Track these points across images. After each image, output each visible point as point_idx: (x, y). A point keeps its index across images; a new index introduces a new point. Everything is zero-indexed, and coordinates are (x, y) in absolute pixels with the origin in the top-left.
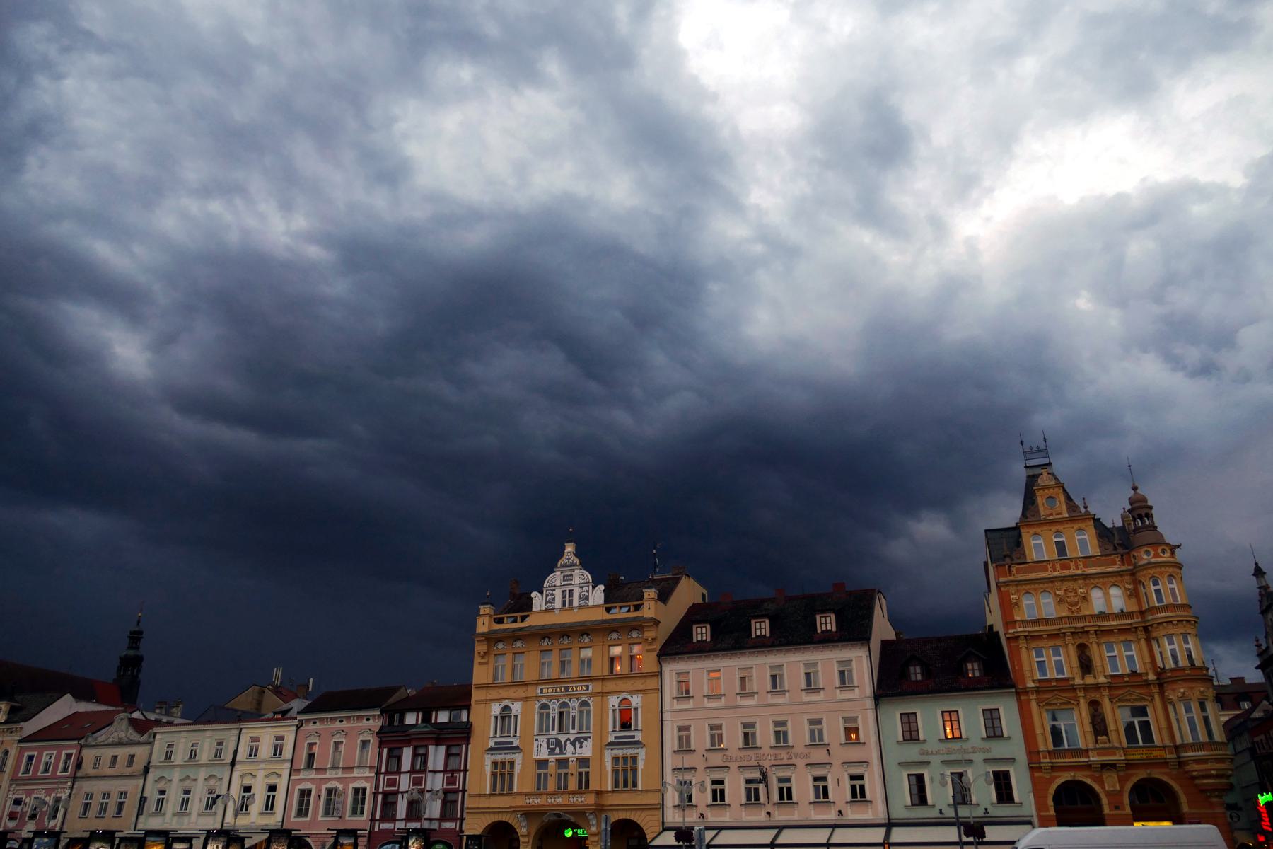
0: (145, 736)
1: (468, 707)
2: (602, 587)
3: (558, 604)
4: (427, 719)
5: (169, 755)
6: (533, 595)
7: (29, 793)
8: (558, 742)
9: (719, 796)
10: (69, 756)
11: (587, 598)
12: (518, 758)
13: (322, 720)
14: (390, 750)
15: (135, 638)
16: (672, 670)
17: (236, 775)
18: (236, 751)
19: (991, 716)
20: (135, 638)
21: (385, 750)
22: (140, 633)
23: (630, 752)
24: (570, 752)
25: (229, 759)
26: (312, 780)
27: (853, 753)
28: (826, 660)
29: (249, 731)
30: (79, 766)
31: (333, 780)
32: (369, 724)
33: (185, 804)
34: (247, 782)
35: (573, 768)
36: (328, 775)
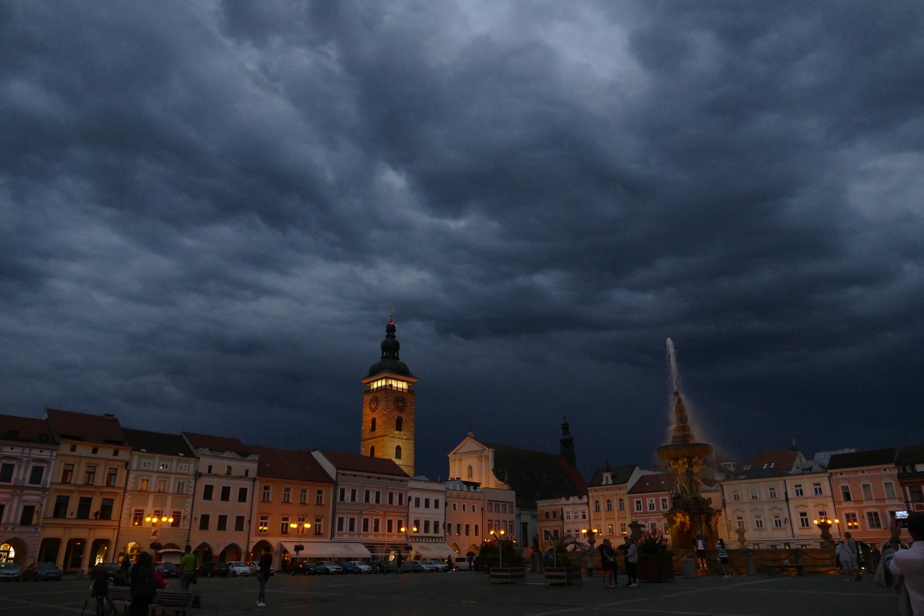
0: (714, 488)
5: (737, 497)
7: (646, 521)
10: (664, 500)
13: (847, 472)
14: (910, 487)
15: (565, 428)
17: (792, 507)
20: (565, 428)
21: (907, 488)
22: (567, 424)
25: (783, 497)
26: (853, 508)
29: (791, 483)
32: (889, 473)
33: (759, 524)
34: (803, 510)
36: (865, 504)
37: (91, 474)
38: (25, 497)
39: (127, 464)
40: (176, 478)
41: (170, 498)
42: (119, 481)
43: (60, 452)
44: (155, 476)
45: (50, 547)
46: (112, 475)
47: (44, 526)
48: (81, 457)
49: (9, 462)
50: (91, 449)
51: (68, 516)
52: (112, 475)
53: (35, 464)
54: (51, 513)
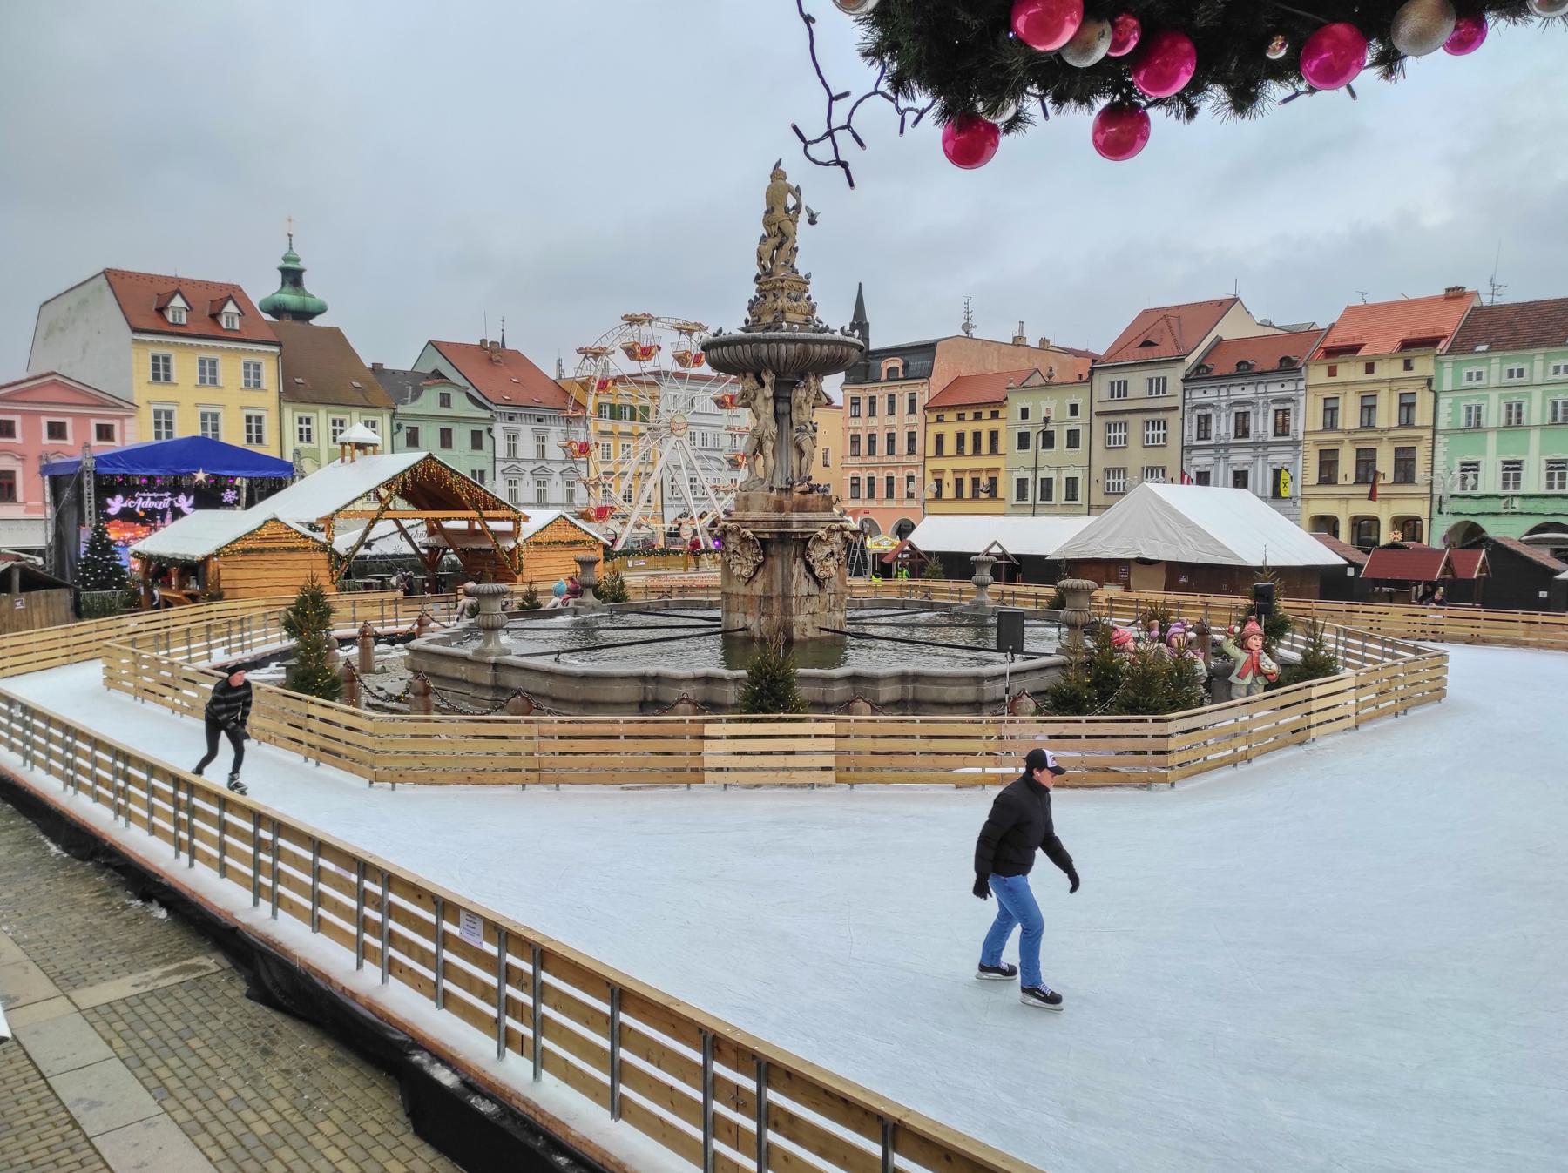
37: (1368, 408)
38: (1272, 458)
39: (1430, 381)
40: (1545, 395)
41: (1535, 436)
42: (1422, 415)
43: (1311, 383)
44: (1494, 396)
45: (1364, 529)
46: (1407, 406)
47: (1306, 498)
48: (1345, 384)
49: (1242, 409)
50: (1362, 367)
51: (1341, 481)
52: (1407, 406)
53: (1277, 406)
54: (1313, 477)
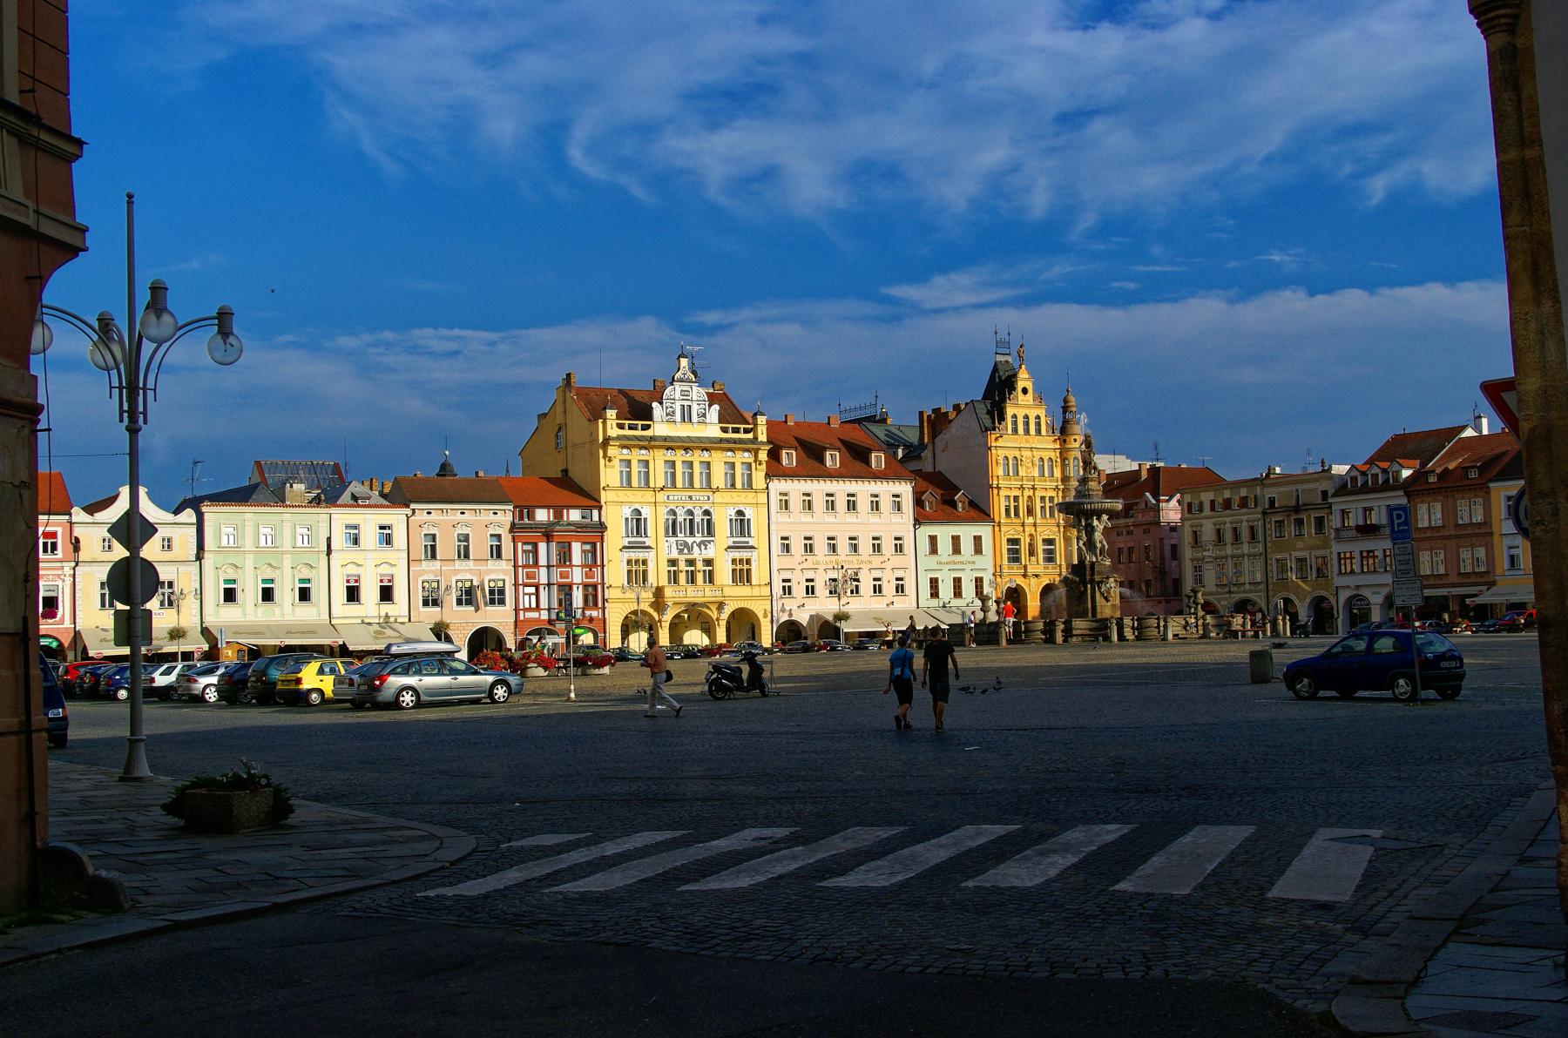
1: (600, 508)
2: (716, 407)
3: (678, 417)
4: (558, 515)
6: (655, 405)
8: (686, 544)
9: (810, 591)
11: (704, 415)
12: (650, 556)
16: (778, 486)
18: (329, 539)
19: (978, 540)
23: (744, 554)
24: (696, 554)
27: (898, 560)
28: (885, 489)
30: (77, 548)
31: (466, 572)
35: (700, 566)
